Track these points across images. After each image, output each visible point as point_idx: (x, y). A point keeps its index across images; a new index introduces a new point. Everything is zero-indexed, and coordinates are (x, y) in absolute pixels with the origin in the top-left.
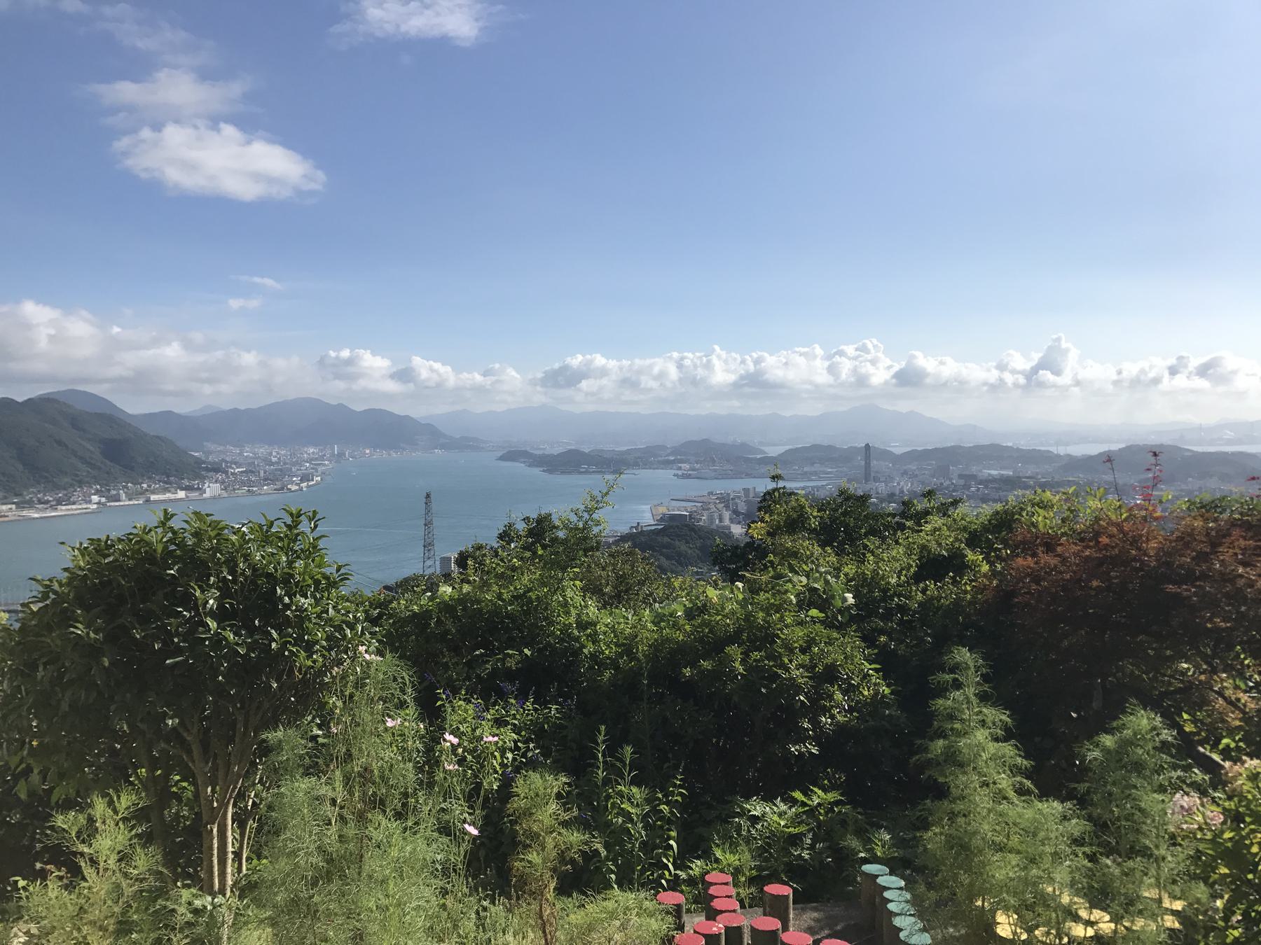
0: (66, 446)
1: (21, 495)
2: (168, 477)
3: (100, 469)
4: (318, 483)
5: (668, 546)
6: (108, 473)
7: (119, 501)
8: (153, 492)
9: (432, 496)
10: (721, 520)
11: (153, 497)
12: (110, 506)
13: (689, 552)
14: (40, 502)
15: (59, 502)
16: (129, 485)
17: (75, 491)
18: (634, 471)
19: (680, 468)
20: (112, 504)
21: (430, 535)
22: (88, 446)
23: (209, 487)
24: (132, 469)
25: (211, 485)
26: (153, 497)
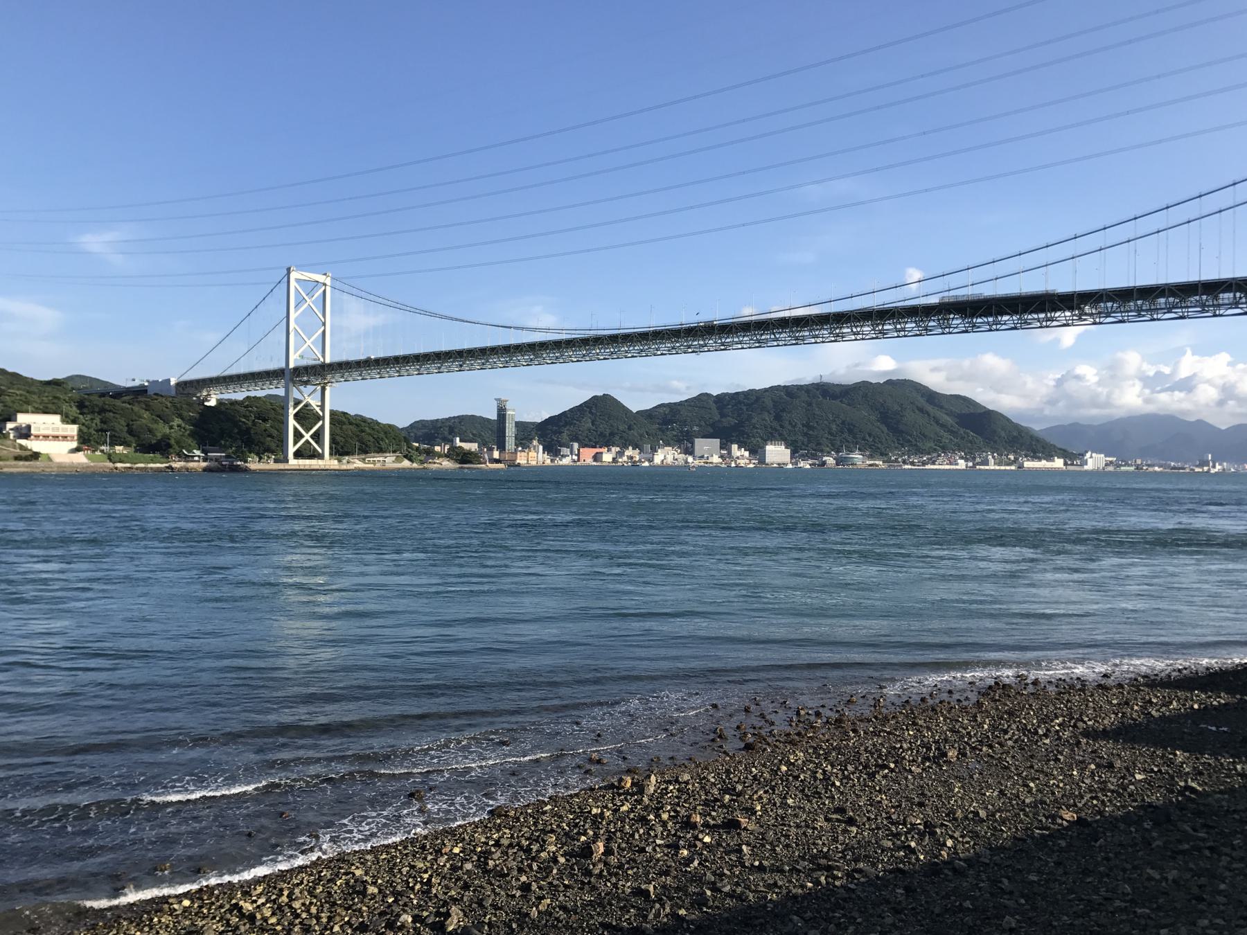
0: (929, 415)
1: (887, 455)
2: (1035, 452)
6: (971, 442)
7: (988, 465)
15: (924, 464)
17: (939, 455)
23: (1091, 457)
25: (1094, 455)
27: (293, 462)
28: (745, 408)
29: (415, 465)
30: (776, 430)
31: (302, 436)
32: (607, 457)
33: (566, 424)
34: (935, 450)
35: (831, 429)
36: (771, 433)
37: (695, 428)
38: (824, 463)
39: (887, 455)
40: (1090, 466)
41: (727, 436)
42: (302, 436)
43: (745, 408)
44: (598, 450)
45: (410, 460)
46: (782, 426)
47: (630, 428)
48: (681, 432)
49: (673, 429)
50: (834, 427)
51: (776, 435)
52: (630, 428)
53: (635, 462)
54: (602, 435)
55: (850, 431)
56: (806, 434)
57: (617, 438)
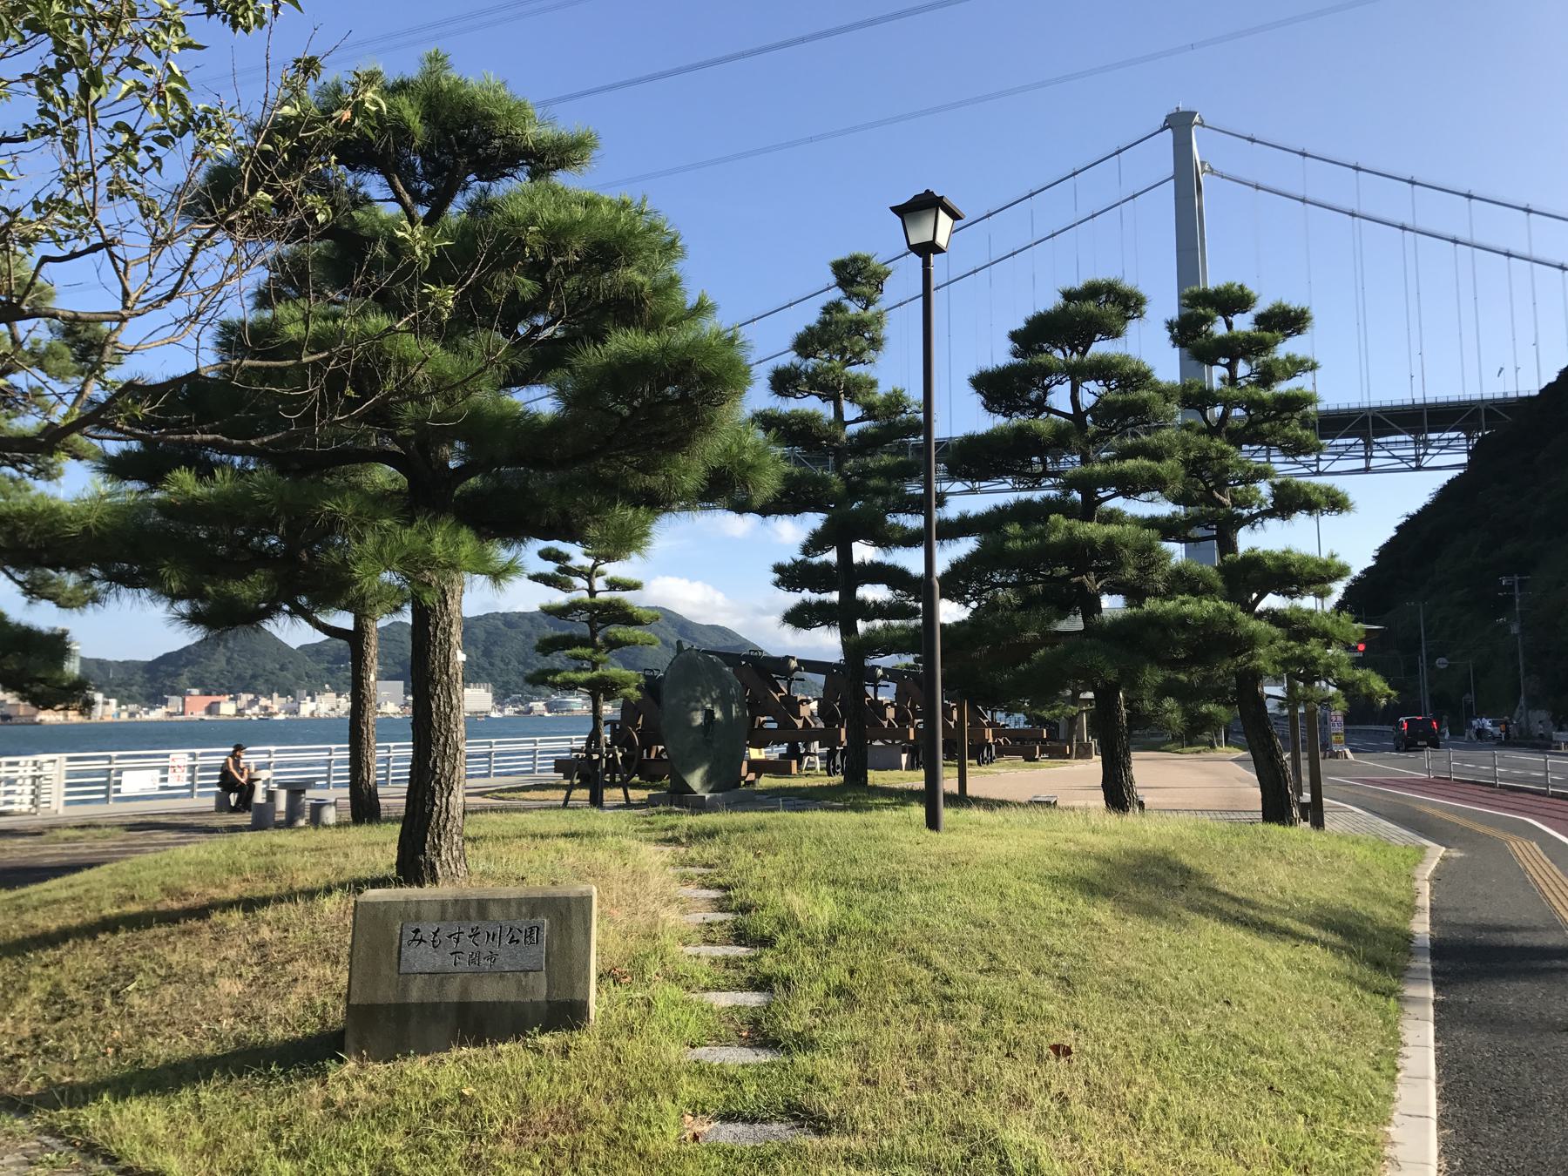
30: (484, 669)
32: (227, 708)
33: (189, 663)
38: (531, 710)
44: (215, 698)
46: (492, 664)
47: (282, 668)
51: (483, 675)
52: (282, 668)
54: (240, 678)
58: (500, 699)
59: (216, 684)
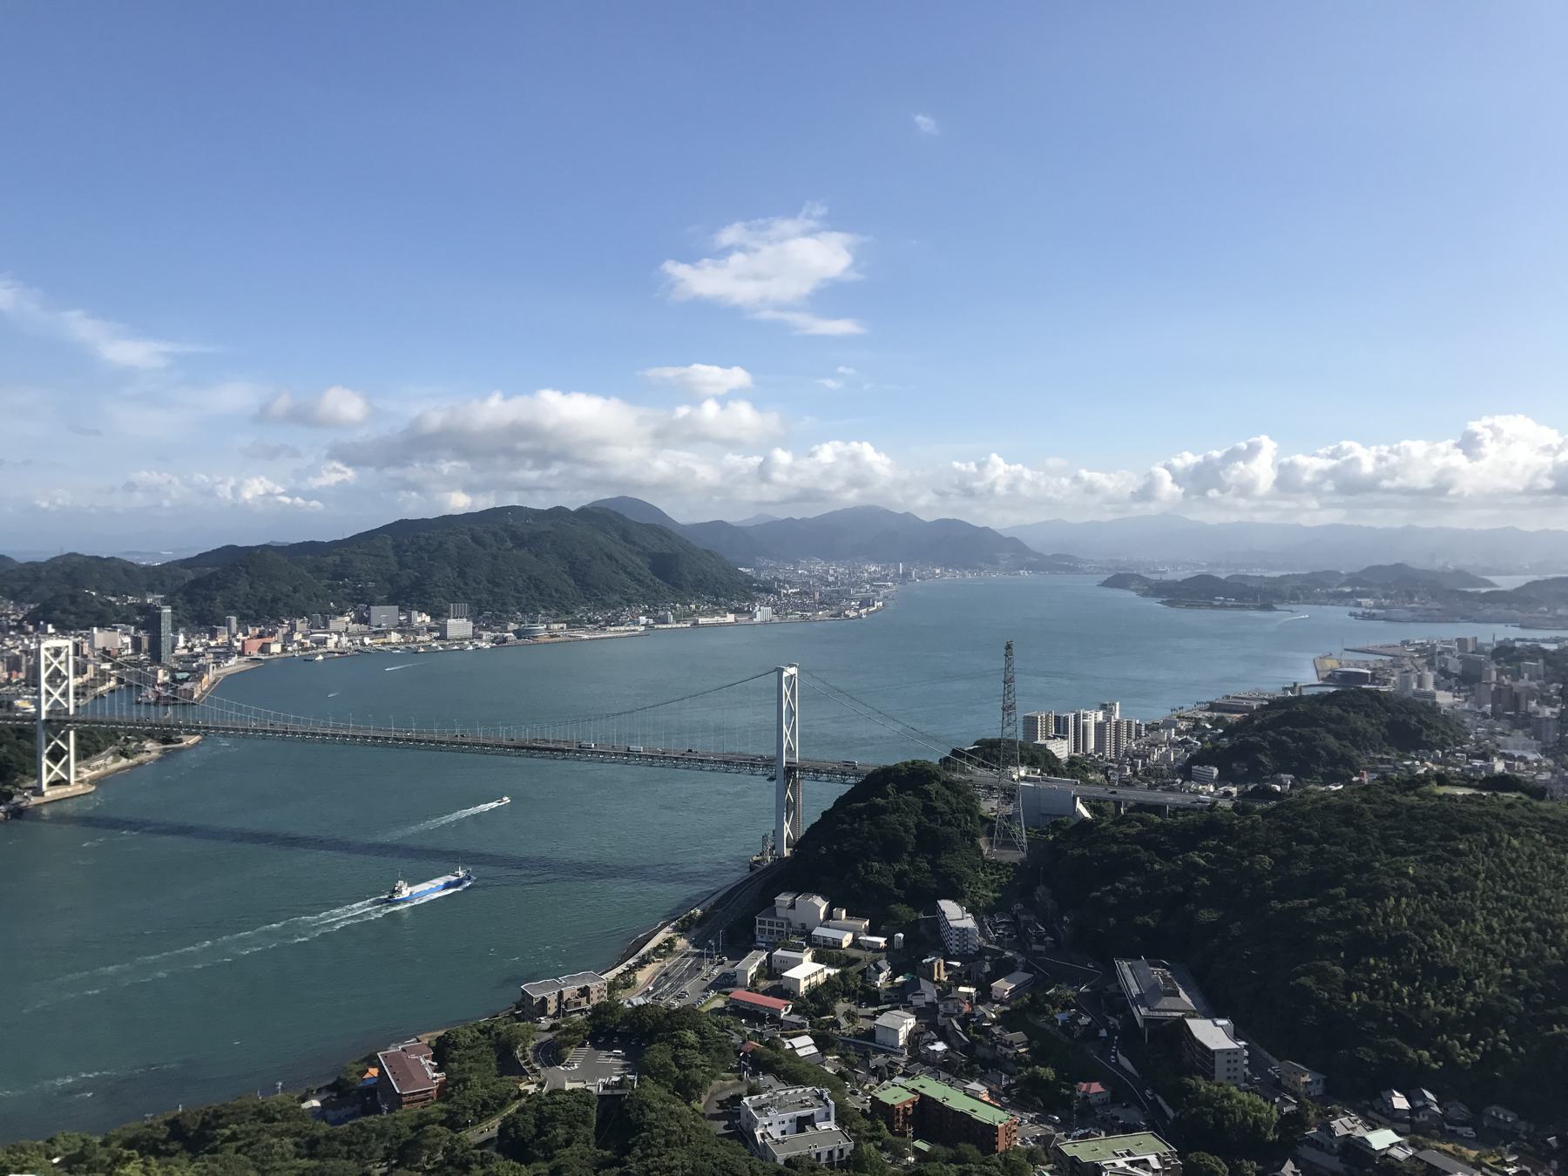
0: (617, 561)
1: (572, 613)
3: (648, 587)
4: (879, 609)
5: (1340, 720)
6: (656, 591)
7: (666, 623)
8: (701, 615)
9: (1014, 647)
10: (1420, 685)
11: (702, 620)
12: (658, 629)
13: (1370, 730)
14: (591, 623)
15: (608, 623)
16: (678, 605)
17: (624, 610)
18: (1294, 608)
19: (1359, 605)
20: (660, 626)
21: (1010, 696)
22: (638, 561)
23: (760, 610)
24: (681, 587)
25: (762, 608)
26: (702, 620)
27: (50, 794)
28: (426, 556)
29: (131, 761)
30: (459, 588)
31: (53, 770)
34: (620, 604)
35: (516, 585)
36: (455, 592)
37: (371, 584)
39: (572, 613)
40: (758, 619)
41: (407, 596)
42: (53, 770)
43: (426, 556)
45: (127, 757)
46: (466, 584)
47: (295, 591)
48: (355, 589)
49: (345, 586)
50: (520, 582)
53: (306, 649)
55: (537, 587)
56: (491, 592)
57: (281, 604)
58: (475, 616)
59: (244, 606)
